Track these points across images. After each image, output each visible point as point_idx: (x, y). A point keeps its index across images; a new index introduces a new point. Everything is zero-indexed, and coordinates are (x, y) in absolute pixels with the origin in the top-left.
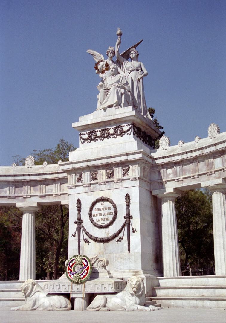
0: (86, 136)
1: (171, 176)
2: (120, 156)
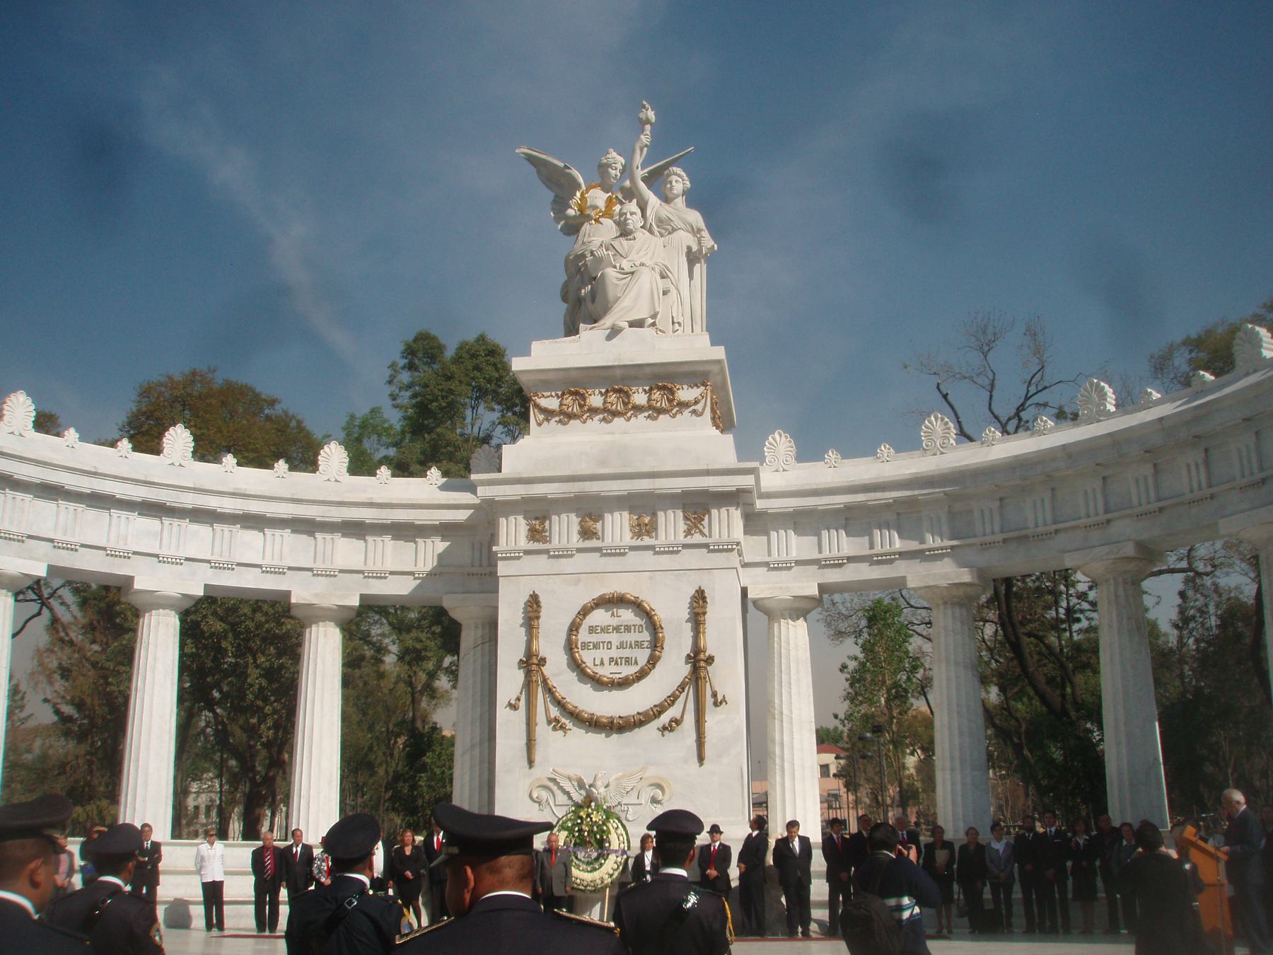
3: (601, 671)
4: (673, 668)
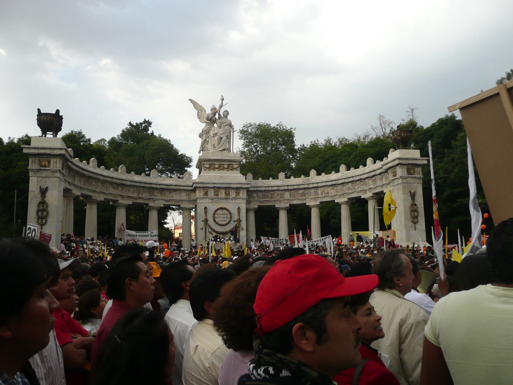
1: (256, 198)
2: (237, 184)
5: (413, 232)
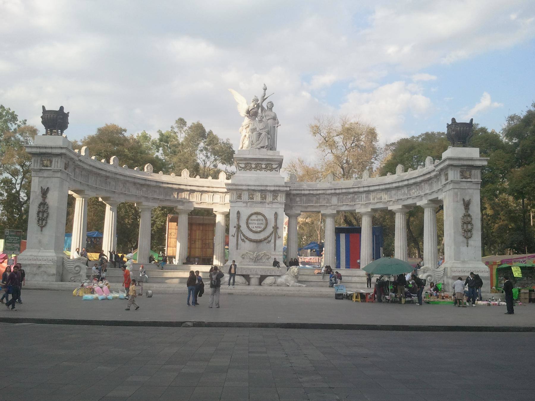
0: (243, 166)
1: (299, 203)
2: (274, 186)
3: (253, 229)
4: (270, 229)
5: (464, 249)
